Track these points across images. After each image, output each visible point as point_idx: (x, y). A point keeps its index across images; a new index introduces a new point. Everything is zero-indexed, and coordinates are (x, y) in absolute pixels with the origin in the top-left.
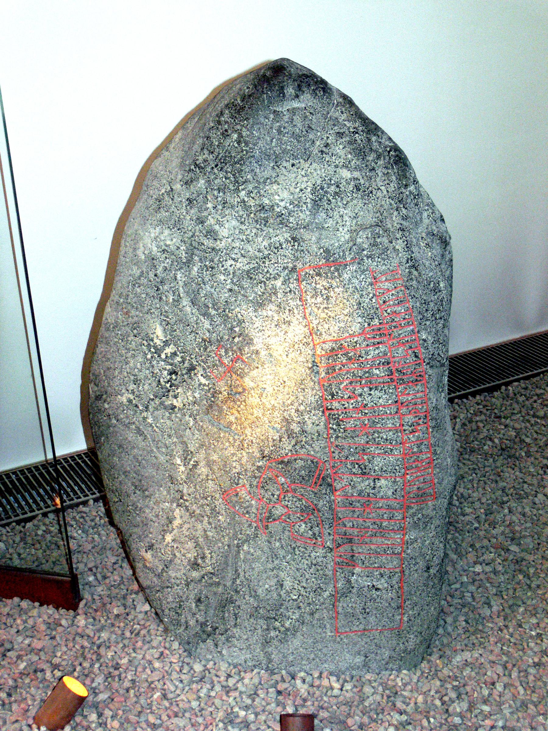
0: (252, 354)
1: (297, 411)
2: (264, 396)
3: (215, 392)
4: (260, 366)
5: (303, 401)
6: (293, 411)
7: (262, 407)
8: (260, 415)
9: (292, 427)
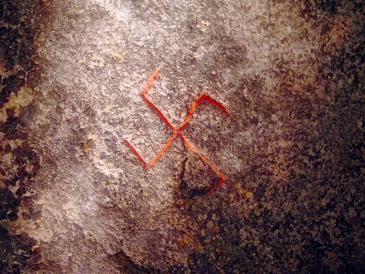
0: (242, 88)
1: (341, 220)
2: (268, 193)
3: (140, 196)
4: (260, 118)
5: (353, 197)
6: (333, 221)
7: (261, 221)
8: (256, 243)
9: (325, 261)
